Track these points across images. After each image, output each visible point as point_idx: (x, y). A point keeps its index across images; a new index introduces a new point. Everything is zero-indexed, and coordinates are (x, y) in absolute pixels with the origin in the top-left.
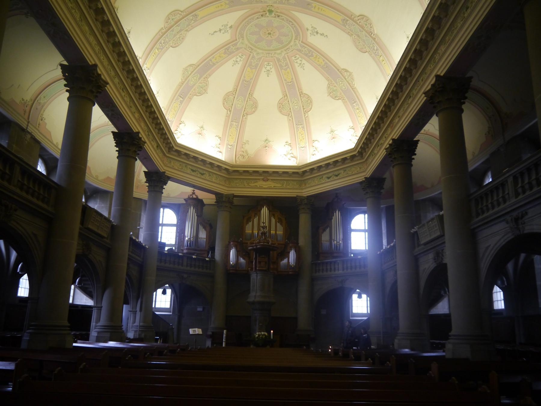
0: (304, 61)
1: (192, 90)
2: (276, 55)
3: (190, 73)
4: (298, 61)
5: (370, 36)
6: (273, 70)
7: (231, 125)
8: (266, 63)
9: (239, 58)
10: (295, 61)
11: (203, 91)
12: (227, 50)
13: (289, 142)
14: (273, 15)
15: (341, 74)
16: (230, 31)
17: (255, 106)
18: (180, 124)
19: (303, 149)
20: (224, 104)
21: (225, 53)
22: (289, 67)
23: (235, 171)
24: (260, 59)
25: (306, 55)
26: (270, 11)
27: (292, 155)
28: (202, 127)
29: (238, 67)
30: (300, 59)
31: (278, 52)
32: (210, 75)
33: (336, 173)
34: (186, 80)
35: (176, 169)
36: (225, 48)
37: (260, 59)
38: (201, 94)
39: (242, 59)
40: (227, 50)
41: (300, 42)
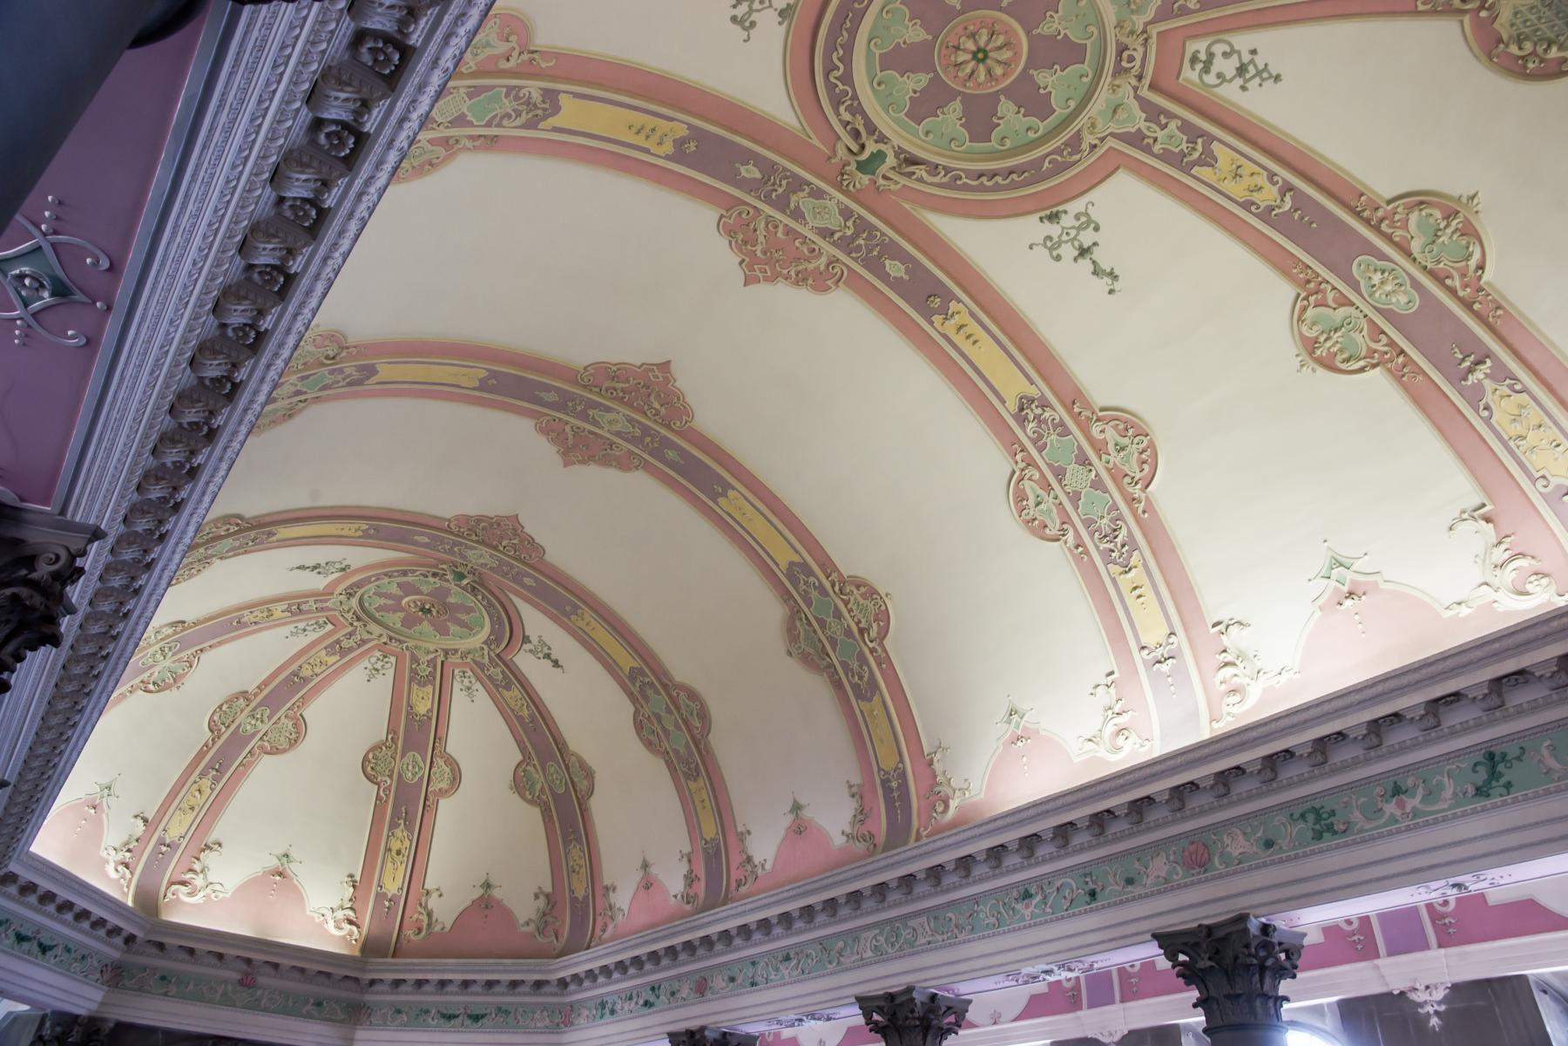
9: (1219, 64)
21: (1208, 160)
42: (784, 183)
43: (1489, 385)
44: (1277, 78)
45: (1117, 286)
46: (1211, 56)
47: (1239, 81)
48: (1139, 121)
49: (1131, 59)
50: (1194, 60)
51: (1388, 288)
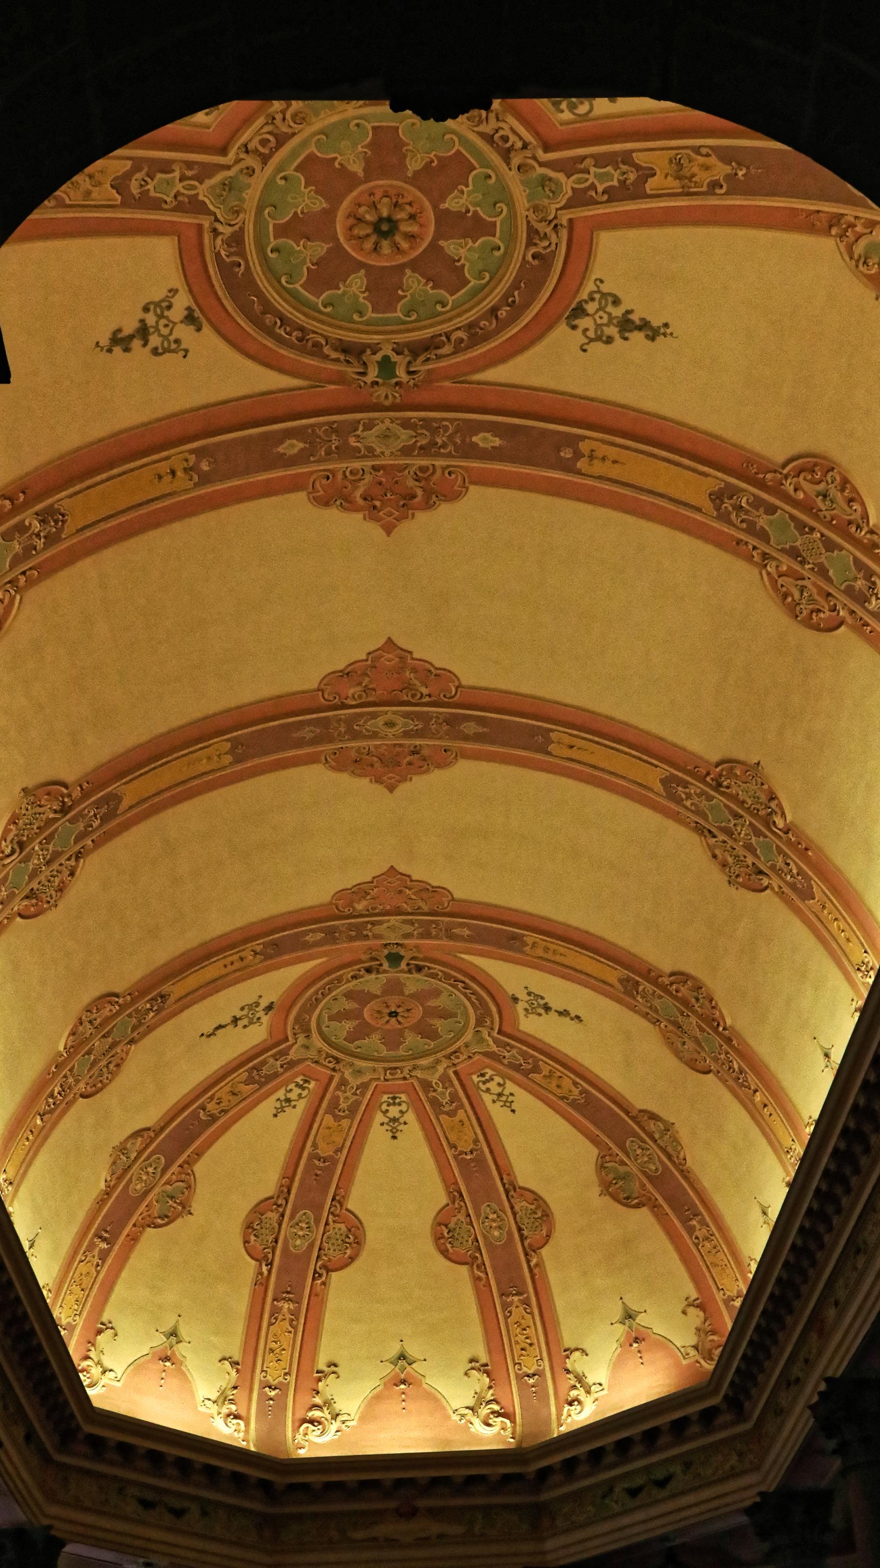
0: (510, 1087)
1: (143, 1207)
2: (418, 1073)
3: (133, 1155)
4: (492, 1085)
5: (715, 1030)
6: (410, 1117)
7: (275, 1311)
8: (385, 1097)
9: (298, 1091)
10: (483, 1087)
11: (176, 1207)
12: (255, 1074)
13: (484, 1359)
14: (403, 965)
15: (638, 1124)
16: (265, 1019)
17: (355, 1238)
18: (99, 1332)
19: (531, 1381)
20: (246, 1242)
22: (462, 1106)
23: (293, 1488)
24: (364, 1086)
25: (517, 1068)
26: (395, 959)
27: (496, 1407)
28: (173, 1333)
29: (293, 1117)
30: (498, 1079)
31: (424, 1062)
32: (199, 1154)
33: (660, 1474)
34: (119, 1179)
35: (87, 1510)
36: (251, 1065)
37: (364, 1086)
38: (168, 1219)
39: (305, 1093)
40: (255, 1074)
41: (495, 1034)
42: (434, 933)
43: (96, 1252)
44: (275, 1116)
45: (204, 1037)
46: (303, 1089)
47: (283, 1098)
48: (293, 1055)
49: (330, 1062)
50: (306, 1081)
51: (144, 1178)
